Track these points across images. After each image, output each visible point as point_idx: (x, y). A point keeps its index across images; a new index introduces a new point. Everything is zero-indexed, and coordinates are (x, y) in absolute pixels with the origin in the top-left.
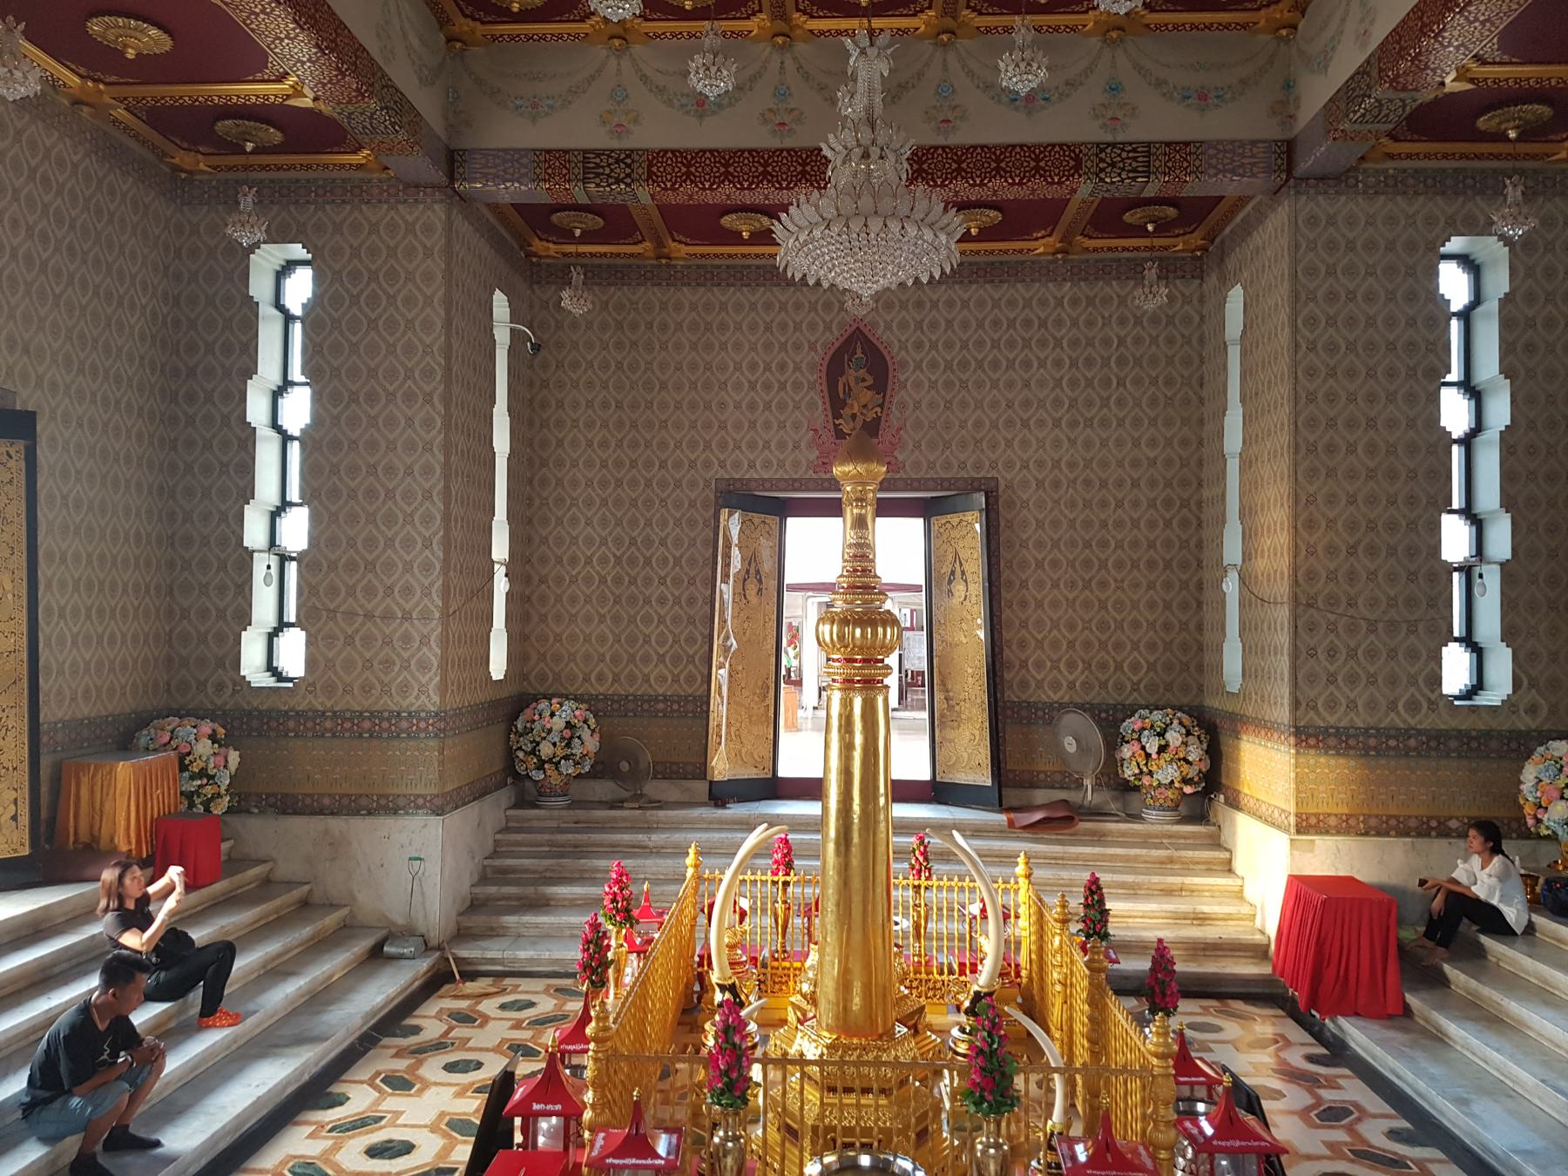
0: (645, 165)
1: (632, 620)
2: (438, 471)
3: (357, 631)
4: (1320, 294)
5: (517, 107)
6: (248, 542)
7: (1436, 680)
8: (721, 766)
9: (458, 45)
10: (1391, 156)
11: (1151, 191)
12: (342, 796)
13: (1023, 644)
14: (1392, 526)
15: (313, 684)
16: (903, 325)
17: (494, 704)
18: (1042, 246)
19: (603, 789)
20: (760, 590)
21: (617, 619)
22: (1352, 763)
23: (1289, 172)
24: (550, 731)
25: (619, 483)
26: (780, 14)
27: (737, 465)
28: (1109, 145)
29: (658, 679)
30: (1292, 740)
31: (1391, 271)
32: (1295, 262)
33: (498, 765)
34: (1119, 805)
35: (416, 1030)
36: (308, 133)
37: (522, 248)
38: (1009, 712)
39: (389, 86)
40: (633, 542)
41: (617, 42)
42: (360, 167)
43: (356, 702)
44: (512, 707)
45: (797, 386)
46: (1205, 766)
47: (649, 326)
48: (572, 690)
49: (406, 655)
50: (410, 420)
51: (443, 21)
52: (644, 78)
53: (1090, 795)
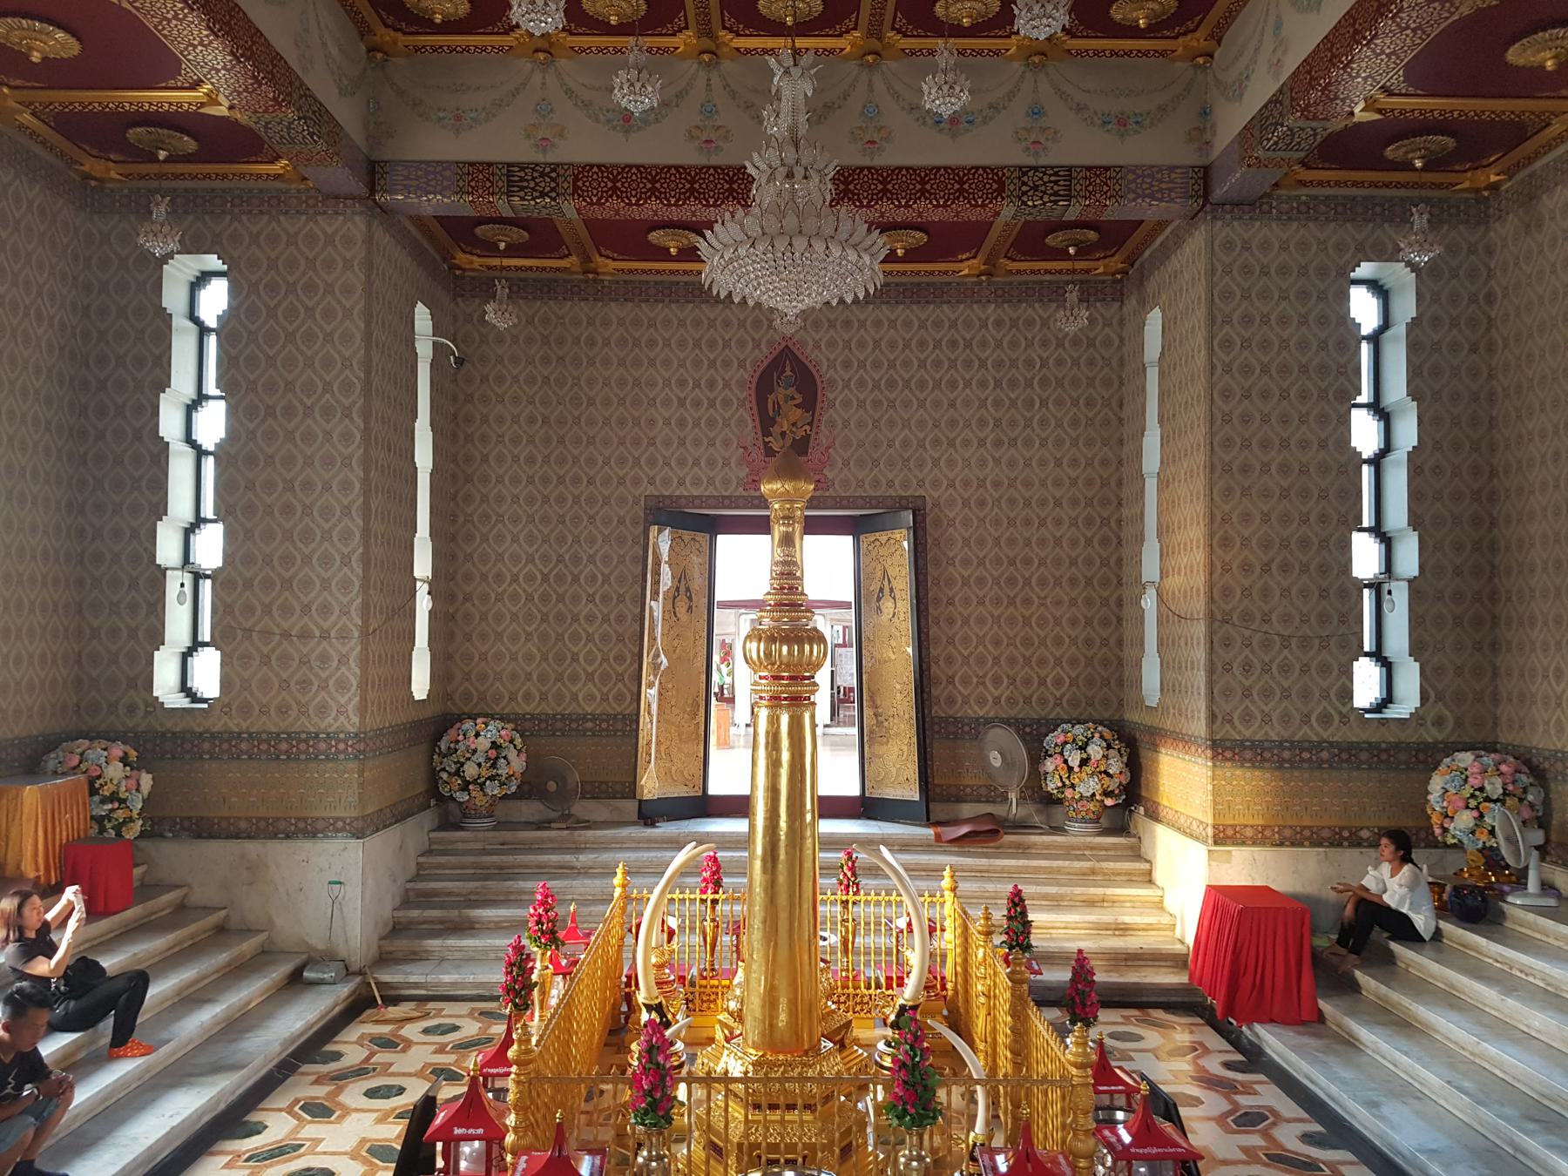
1: (560, 637)
2: (358, 486)
3: (273, 650)
4: (1235, 317)
5: (440, 119)
6: (161, 559)
7: (1347, 694)
8: (651, 785)
9: (379, 55)
10: (1302, 183)
11: (1072, 214)
12: (259, 819)
13: (950, 660)
14: (1304, 544)
15: (229, 705)
16: (832, 344)
17: (416, 725)
18: (966, 268)
19: (530, 809)
20: (690, 607)
21: (544, 637)
22: (1268, 775)
23: (1206, 196)
24: (475, 751)
25: (546, 500)
26: (706, 32)
27: (666, 482)
28: (1031, 168)
29: (587, 698)
30: (1209, 753)
31: (1303, 295)
32: (1211, 287)
33: (421, 787)
34: (1043, 818)
36: (222, 142)
37: (445, 260)
38: (936, 728)
39: (307, 95)
40: (560, 559)
41: (541, 56)
42: (277, 177)
43: (273, 723)
44: (436, 726)
45: (727, 403)
46: (1125, 779)
47: (576, 341)
48: (497, 710)
49: (324, 675)
50: (328, 434)
51: (364, 31)
52: (569, 92)
53: (1014, 808)
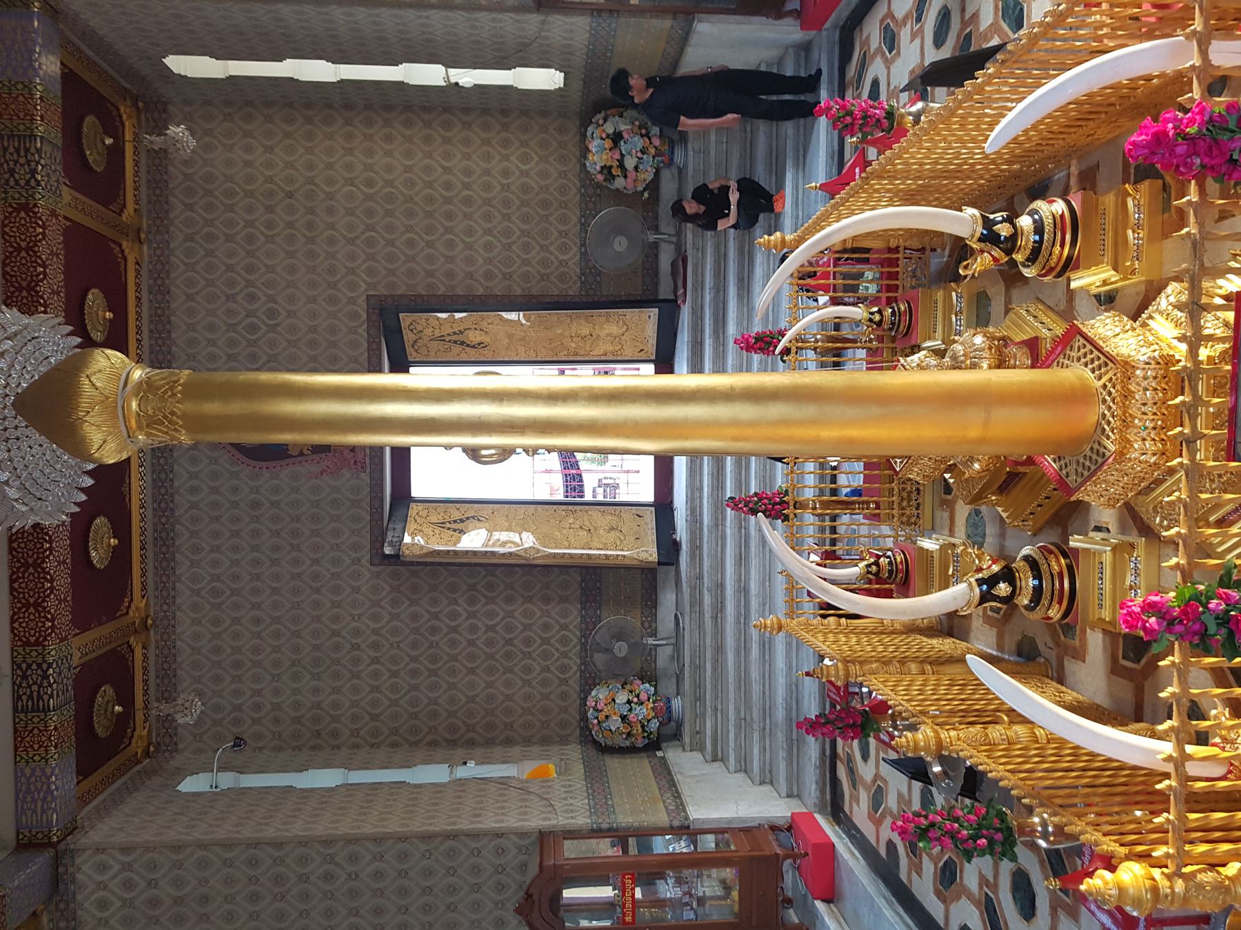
0: (28, 649)
13: (526, 277)
35: (891, 845)
37: (139, 762)
38: (592, 292)
